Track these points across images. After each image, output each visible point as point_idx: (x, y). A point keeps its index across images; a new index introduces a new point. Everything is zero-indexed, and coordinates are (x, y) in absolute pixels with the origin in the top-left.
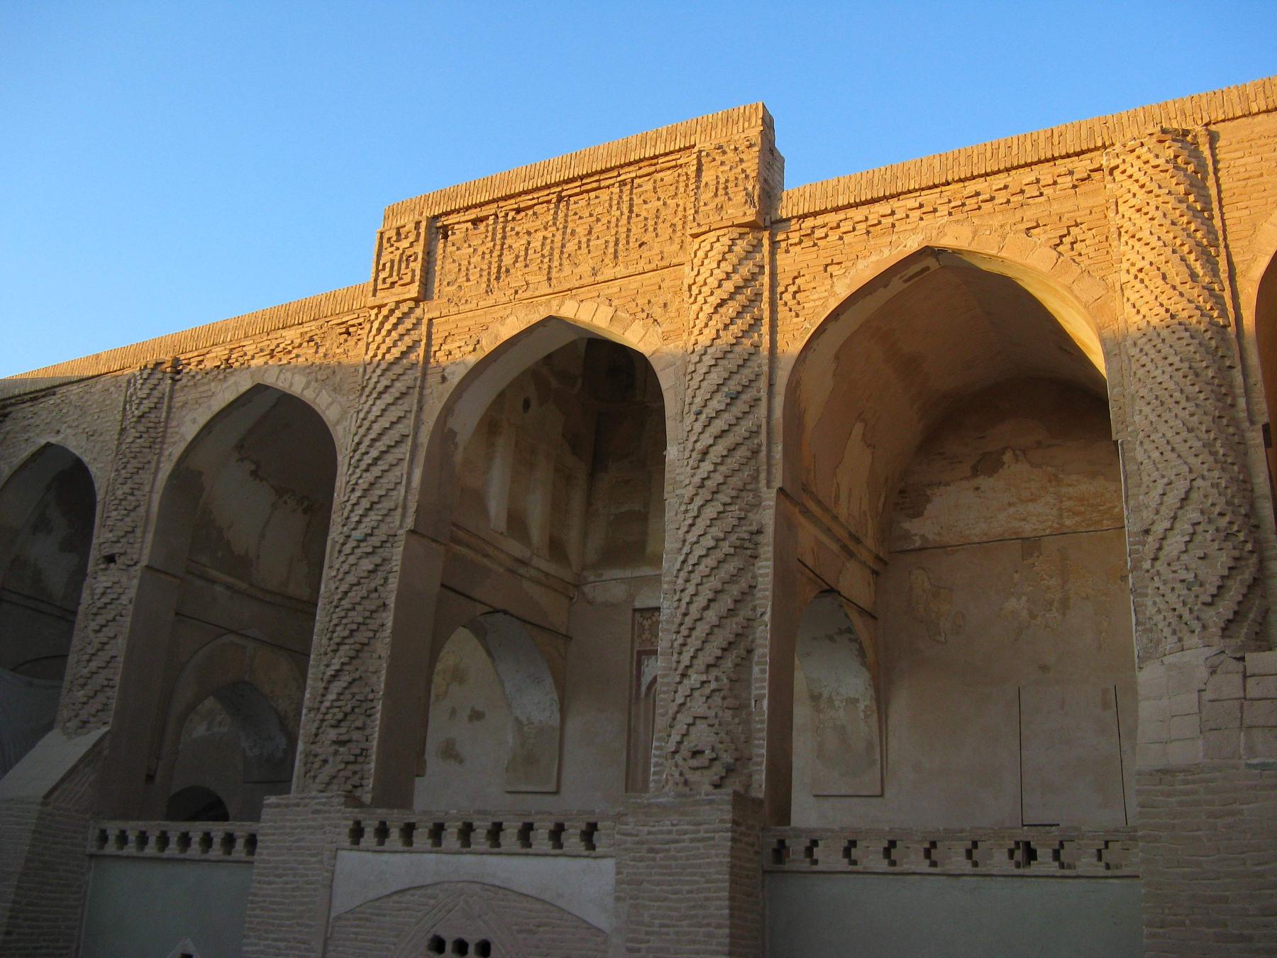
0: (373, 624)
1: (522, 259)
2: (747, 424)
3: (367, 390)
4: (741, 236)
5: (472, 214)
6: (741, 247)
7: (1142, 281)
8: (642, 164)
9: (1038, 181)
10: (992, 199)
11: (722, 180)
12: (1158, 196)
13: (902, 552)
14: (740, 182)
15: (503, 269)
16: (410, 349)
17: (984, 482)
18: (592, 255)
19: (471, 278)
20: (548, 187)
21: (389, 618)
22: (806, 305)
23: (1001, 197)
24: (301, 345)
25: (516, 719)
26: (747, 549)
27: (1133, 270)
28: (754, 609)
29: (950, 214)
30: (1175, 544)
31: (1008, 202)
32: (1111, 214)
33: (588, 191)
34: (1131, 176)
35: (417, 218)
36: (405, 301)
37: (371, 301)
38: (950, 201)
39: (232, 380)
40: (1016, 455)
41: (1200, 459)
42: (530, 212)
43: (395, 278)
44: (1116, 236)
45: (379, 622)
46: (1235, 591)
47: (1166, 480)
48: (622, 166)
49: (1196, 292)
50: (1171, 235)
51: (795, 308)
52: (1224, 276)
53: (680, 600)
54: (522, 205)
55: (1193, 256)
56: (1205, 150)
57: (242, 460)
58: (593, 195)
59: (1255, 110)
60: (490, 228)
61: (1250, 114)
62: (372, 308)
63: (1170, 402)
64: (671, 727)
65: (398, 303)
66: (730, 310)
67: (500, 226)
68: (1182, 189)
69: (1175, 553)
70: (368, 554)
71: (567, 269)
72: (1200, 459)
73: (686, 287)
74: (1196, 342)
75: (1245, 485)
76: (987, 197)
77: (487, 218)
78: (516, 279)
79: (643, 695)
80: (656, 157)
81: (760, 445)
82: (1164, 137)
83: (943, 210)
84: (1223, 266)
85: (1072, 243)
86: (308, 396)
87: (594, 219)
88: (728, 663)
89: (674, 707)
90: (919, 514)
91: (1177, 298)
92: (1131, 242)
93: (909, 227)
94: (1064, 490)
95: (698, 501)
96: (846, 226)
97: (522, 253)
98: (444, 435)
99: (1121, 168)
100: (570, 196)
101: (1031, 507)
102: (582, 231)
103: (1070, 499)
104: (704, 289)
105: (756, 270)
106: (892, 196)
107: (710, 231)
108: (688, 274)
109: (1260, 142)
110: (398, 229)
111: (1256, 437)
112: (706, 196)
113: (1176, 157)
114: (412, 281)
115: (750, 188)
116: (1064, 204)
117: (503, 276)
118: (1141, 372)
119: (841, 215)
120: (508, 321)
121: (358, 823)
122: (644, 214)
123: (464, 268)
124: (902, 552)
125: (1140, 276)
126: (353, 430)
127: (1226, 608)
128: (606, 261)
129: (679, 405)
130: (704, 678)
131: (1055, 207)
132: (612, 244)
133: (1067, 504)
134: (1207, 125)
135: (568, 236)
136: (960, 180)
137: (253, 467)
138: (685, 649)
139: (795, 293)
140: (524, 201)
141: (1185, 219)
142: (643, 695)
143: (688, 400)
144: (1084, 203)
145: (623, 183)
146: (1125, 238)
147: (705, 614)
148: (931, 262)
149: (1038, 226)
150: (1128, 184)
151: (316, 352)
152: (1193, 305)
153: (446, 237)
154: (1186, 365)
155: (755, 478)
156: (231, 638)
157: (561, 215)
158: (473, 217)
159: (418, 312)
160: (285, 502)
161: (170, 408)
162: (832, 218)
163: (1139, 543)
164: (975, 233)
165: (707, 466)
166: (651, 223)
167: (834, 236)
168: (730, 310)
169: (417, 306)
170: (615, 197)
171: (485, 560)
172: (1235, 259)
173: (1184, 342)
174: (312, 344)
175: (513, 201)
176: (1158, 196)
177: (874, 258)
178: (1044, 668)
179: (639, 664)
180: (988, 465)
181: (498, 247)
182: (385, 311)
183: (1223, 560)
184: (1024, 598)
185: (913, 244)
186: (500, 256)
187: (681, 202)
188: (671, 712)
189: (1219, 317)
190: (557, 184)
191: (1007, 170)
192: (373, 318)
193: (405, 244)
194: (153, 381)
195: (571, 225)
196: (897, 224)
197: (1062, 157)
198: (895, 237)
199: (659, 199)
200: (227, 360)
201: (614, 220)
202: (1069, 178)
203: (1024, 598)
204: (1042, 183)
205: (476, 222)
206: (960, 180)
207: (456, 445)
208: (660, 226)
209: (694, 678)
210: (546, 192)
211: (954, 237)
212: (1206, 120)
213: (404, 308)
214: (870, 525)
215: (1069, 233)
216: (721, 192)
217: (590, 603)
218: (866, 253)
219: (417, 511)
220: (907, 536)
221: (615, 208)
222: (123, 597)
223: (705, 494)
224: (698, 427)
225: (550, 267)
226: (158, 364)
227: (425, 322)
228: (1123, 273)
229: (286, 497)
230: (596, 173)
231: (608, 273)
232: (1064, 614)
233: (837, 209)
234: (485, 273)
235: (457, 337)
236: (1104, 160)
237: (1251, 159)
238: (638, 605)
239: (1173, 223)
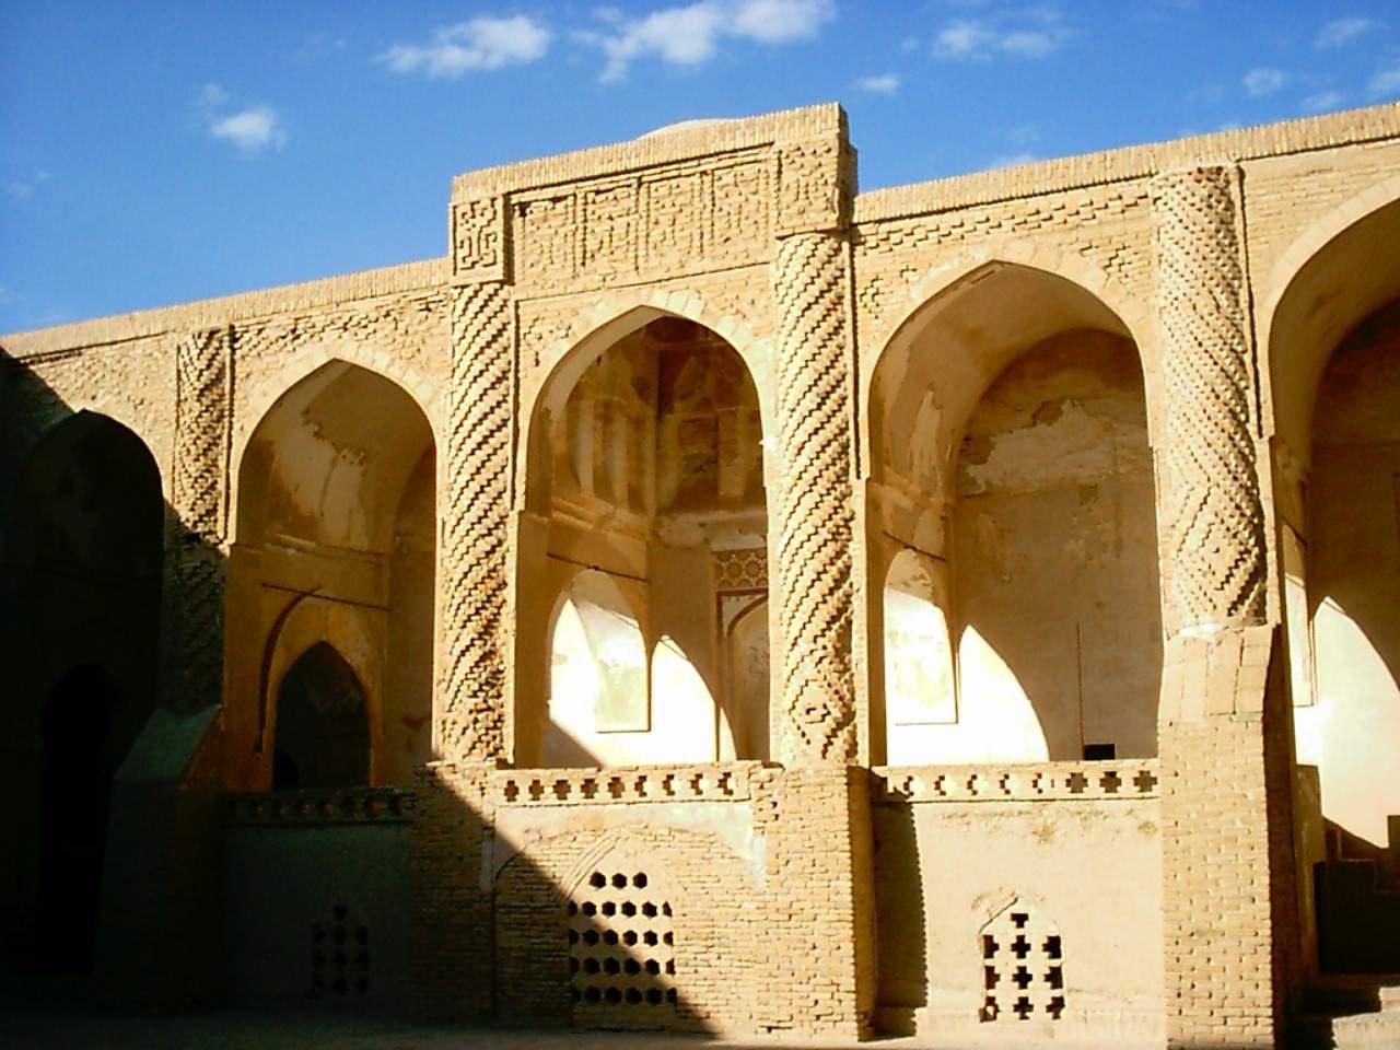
0: (497, 601)
1: (606, 245)
2: (837, 420)
3: (460, 373)
4: (823, 240)
5: (551, 193)
6: (824, 249)
7: (1177, 308)
8: (721, 156)
9: (1092, 203)
10: (1051, 218)
11: (803, 184)
12: (1193, 233)
13: (968, 497)
14: (820, 187)
15: (589, 255)
16: (500, 332)
17: (1042, 428)
18: (678, 247)
19: (556, 261)
20: (627, 172)
21: (510, 594)
22: (886, 309)
23: (1059, 216)
24: (377, 321)
25: (601, 662)
26: (840, 535)
27: (1171, 298)
28: (851, 585)
29: (1014, 230)
30: (1193, 541)
31: (1065, 222)
32: (1153, 242)
33: (668, 179)
34: (1171, 209)
35: (491, 194)
36: (488, 283)
37: (454, 281)
38: (1013, 217)
39: (300, 352)
40: (1074, 405)
41: (1216, 470)
42: (611, 195)
43: (475, 257)
44: (1157, 263)
45: (500, 599)
46: (1240, 577)
47: (1189, 487)
48: (703, 157)
49: (1220, 322)
50: (1202, 270)
51: (874, 309)
52: (1244, 305)
53: (786, 578)
54: (602, 188)
55: (1219, 289)
56: (1234, 189)
57: (307, 423)
58: (674, 182)
59: (1278, 151)
60: (570, 209)
61: (1275, 155)
62: (456, 288)
63: (1194, 419)
64: (787, 687)
65: (482, 284)
66: (817, 312)
67: (580, 208)
68: (1213, 226)
69: (1195, 548)
70: (483, 536)
71: (654, 261)
72: (1216, 470)
73: (772, 285)
74: (1218, 368)
75: (1251, 492)
76: (1047, 216)
77: (565, 198)
78: (602, 264)
79: (725, 635)
80: (735, 151)
81: (848, 440)
82: (1199, 176)
83: (1007, 225)
85: (1120, 265)
86: (393, 374)
87: (677, 209)
88: (832, 634)
89: (787, 671)
90: (984, 461)
91: (1204, 328)
92: (1169, 270)
93: (978, 239)
94: (1118, 439)
95: (797, 492)
96: (919, 234)
97: (607, 239)
98: (540, 415)
99: (1164, 200)
100: (650, 182)
102: (665, 221)
103: (1123, 447)
104: (790, 291)
105: (838, 273)
106: (962, 208)
107: (793, 235)
108: (773, 273)
109: (1281, 181)
110: (473, 204)
111: (1262, 448)
112: (788, 197)
113: (1210, 196)
114: (494, 263)
115: (829, 194)
116: (1112, 227)
117: (588, 262)
118: (1173, 389)
119: (915, 221)
120: (598, 307)
121: (511, 783)
122: (726, 208)
123: (546, 250)
124: (968, 497)
125: (1176, 303)
126: (450, 411)
127: (1233, 590)
128: (693, 254)
129: (772, 401)
130: (813, 646)
131: (1107, 231)
132: (697, 237)
134: (1239, 161)
135: (651, 226)
136: (1024, 197)
137: (317, 429)
138: (793, 621)
139: (874, 295)
140: (604, 184)
141: (1214, 255)
142: (725, 635)
143: (782, 397)
144: (1132, 227)
145: (704, 173)
146: (1164, 265)
147: (810, 591)
148: (998, 268)
149: (1090, 247)
150: (1169, 216)
151: (396, 328)
152: (1216, 335)
153: (523, 214)
154: (1209, 388)
155: (846, 471)
157: (643, 202)
158: (551, 196)
159: (503, 294)
160: (344, 457)
161: (233, 378)
162: (907, 224)
163: (1168, 535)
164: (1036, 250)
165: (803, 460)
166: (734, 218)
167: (909, 241)
168: (817, 312)
169: (502, 288)
170: (697, 188)
171: (579, 522)
172: (1253, 290)
173: (1208, 368)
174: (389, 319)
175: (592, 182)
176: (1193, 233)
177: (946, 267)
178: (1099, 605)
179: (719, 604)
180: (1046, 413)
181: (581, 231)
182: (469, 292)
183: (1230, 553)
184: (1082, 541)
185: (981, 258)
186: (584, 240)
187: (763, 200)
188: (785, 676)
189: (1239, 344)
190: (636, 170)
191: (1065, 190)
192: (456, 296)
193: (480, 221)
194: (211, 350)
195: (653, 213)
196: (966, 235)
197: (1113, 182)
198: (964, 248)
199: (740, 194)
200: (294, 331)
201: (697, 212)
202: (1119, 202)
203: (1082, 541)
204: (1095, 206)
205: (556, 200)
206: (1024, 197)
207: (551, 421)
208: (743, 222)
209: (804, 646)
210: (627, 176)
211: (1019, 253)
212: (1238, 157)
213: (489, 289)
214: (939, 478)
215: (1117, 256)
216: (802, 196)
217: (667, 546)
218: (938, 261)
219: (526, 493)
220: (973, 482)
221: (697, 199)
222: (215, 576)
223: (803, 486)
224: (793, 424)
225: (636, 257)
226: (212, 333)
227: (511, 304)
228: (1161, 299)
229: (345, 452)
230: (677, 162)
231: (694, 265)
232: (1118, 556)
233: (911, 216)
234: (570, 257)
235: (547, 321)
236: (1146, 186)
237: (1272, 197)
238: (716, 546)
239: (1204, 258)
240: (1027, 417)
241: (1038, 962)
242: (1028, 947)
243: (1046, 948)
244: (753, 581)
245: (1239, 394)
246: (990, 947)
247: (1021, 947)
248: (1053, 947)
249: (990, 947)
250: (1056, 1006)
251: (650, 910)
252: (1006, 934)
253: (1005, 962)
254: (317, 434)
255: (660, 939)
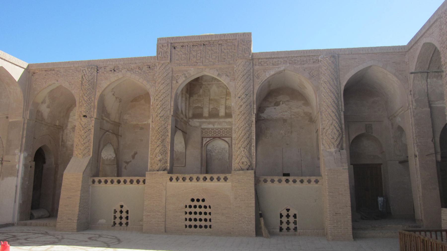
17: (277, 108)
30: (329, 131)
84: (339, 83)
101: (286, 113)
127: (337, 143)
133: (292, 113)
156: (107, 133)
178: (287, 144)
179: (202, 140)
217: (191, 126)
220: (261, 117)
238: (202, 127)
240: (273, 104)
241: (291, 219)
242: (290, 216)
243: (293, 216)
244: (224, 135)
245: (338, 101)
246: (281, 216)
247: (288, 216)
248: (295, 216)
249: (281, 216)
250: (295, 229)
251: (205, 207)
252: (285, 213)
253: (285, 219)
254: (113, 94)
255: (208, 214)
